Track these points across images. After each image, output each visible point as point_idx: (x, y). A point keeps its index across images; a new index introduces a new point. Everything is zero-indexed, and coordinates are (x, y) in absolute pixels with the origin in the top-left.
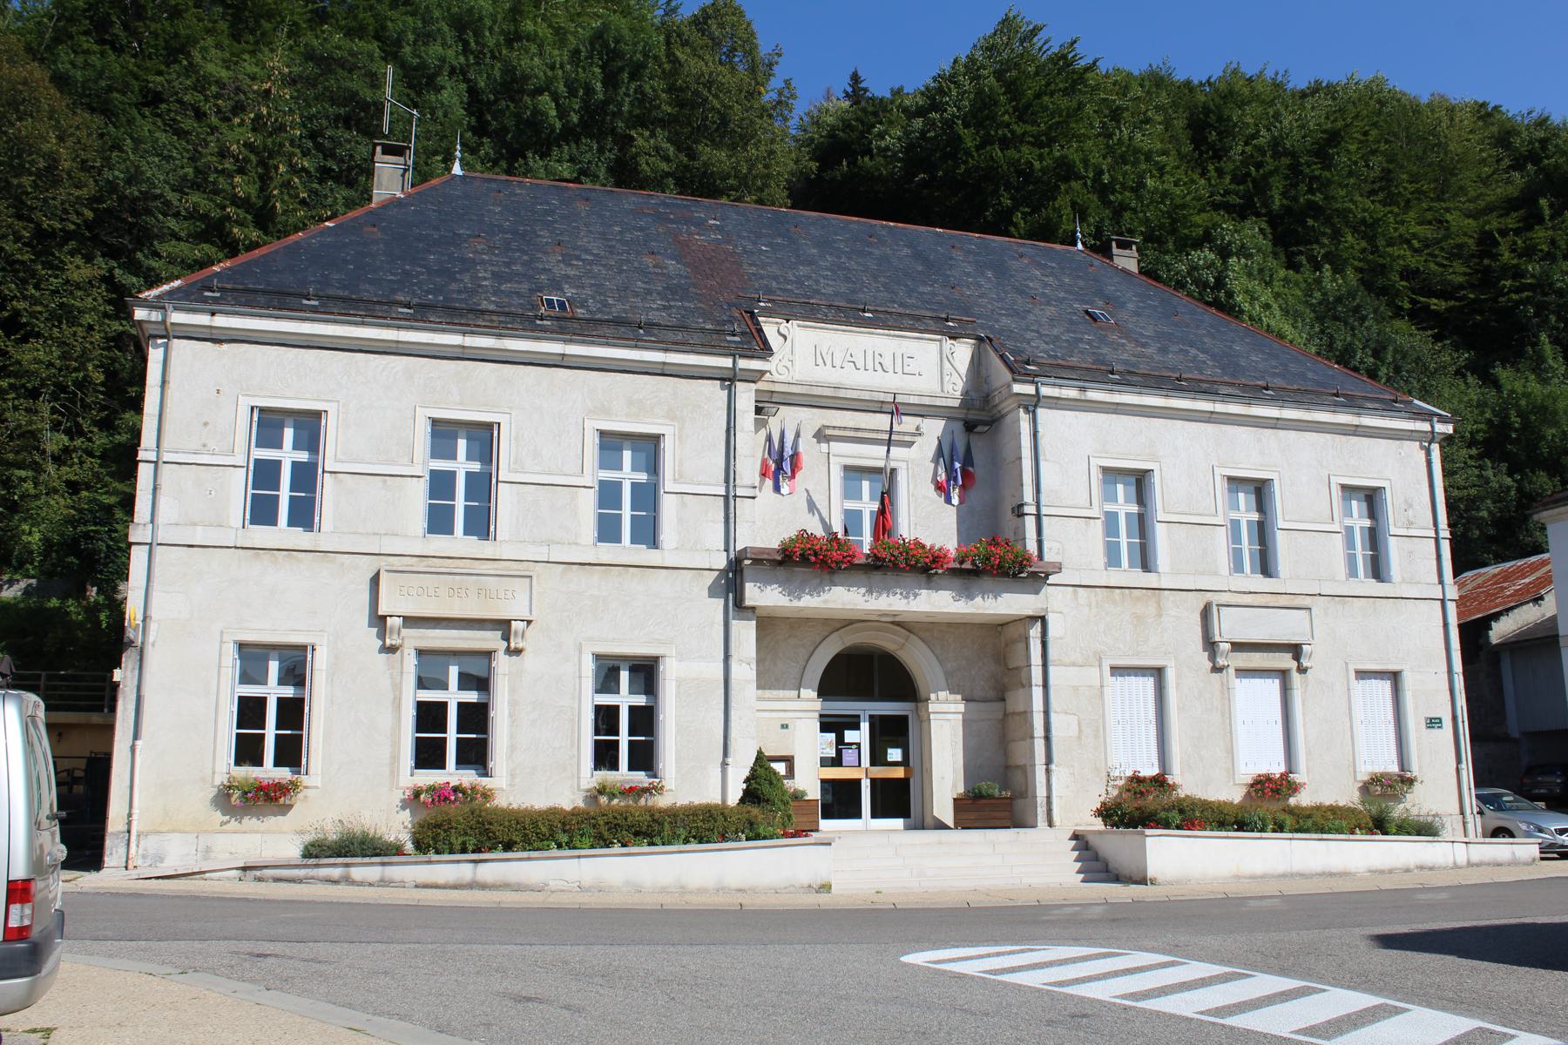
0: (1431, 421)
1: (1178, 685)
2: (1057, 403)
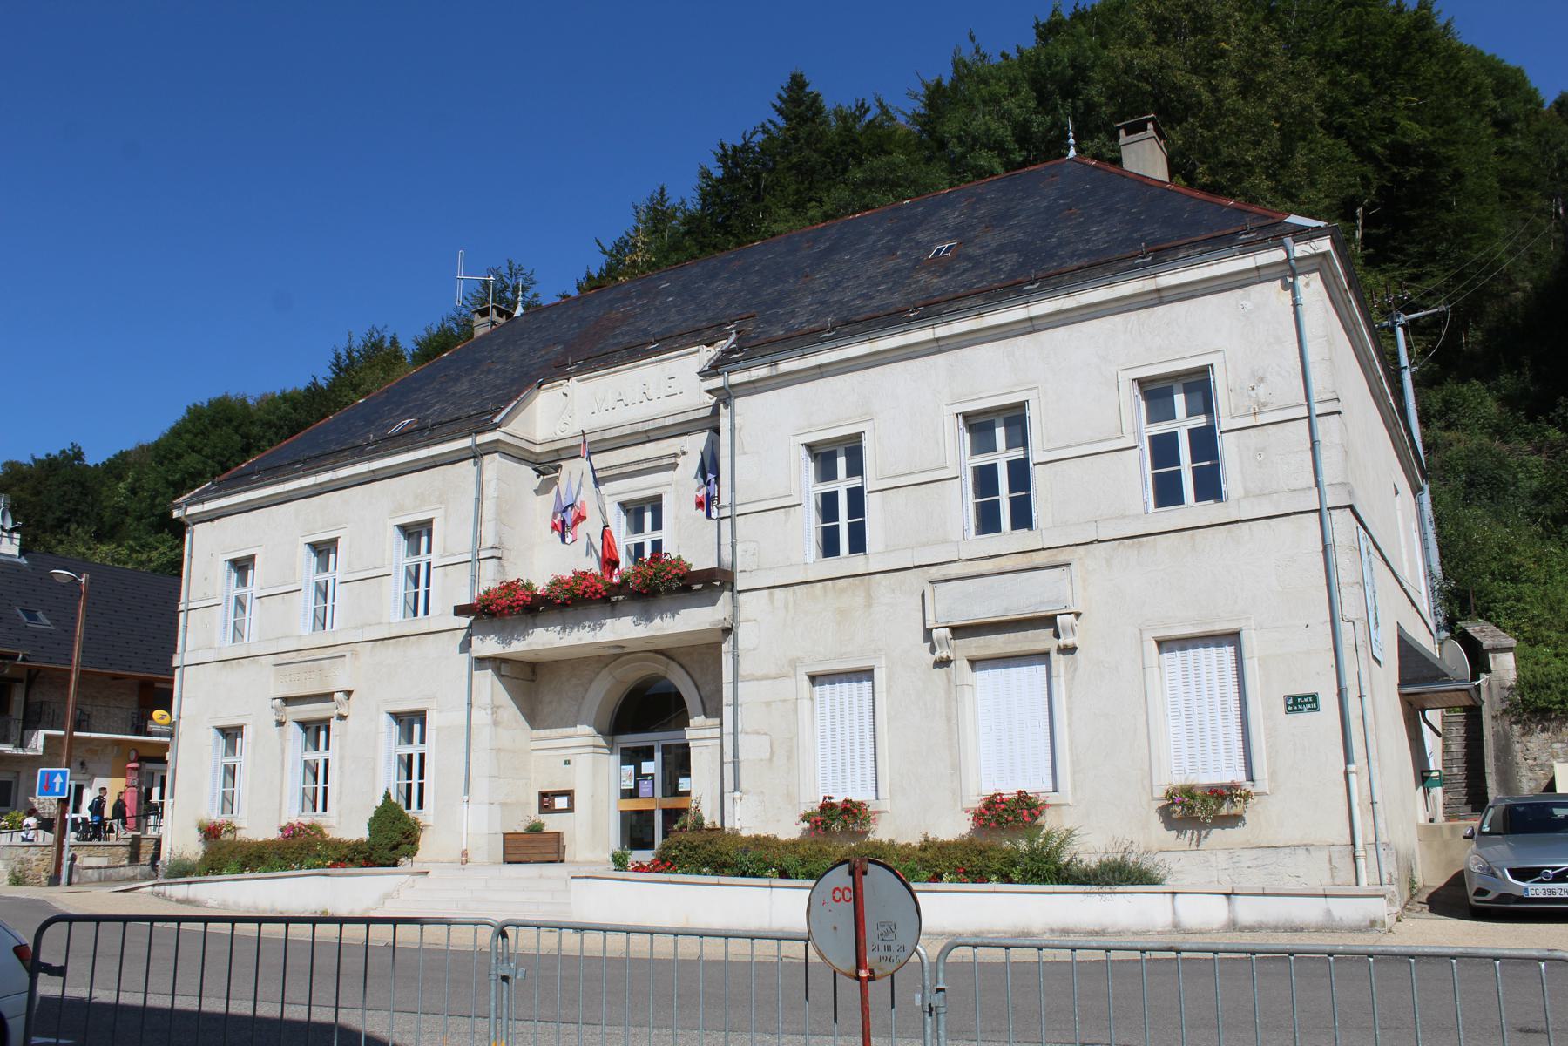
0: (1283, 245)
1: (888, 690)
2: (752, 388)
